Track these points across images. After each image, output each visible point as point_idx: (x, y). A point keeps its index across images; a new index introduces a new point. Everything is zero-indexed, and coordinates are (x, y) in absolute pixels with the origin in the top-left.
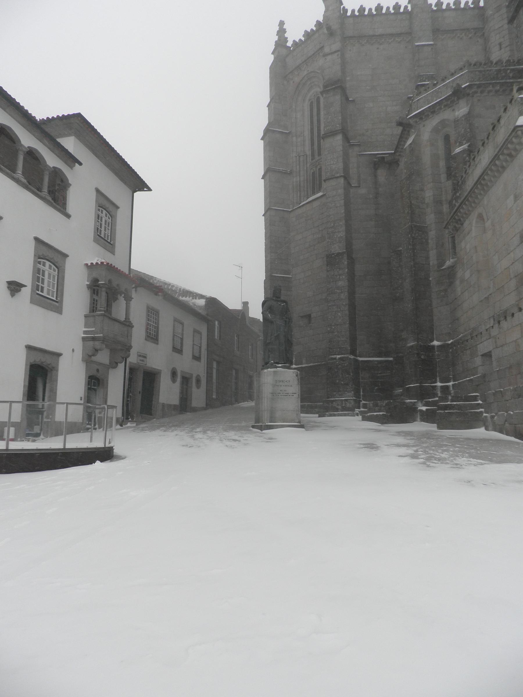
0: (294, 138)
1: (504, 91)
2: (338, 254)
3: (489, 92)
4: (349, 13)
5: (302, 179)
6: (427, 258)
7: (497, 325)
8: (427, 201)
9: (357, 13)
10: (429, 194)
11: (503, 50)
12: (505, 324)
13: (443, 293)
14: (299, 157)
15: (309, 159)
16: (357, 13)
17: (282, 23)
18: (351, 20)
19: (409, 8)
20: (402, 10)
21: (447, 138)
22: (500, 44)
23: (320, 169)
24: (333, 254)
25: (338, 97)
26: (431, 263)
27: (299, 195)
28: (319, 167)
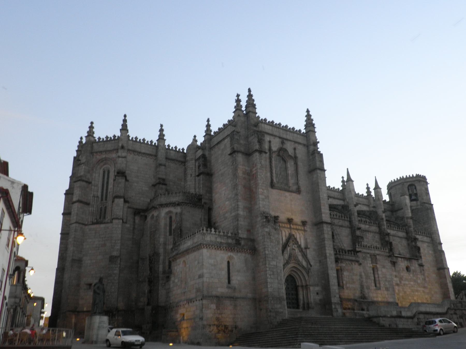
0: (93, 187)
1: (193, 207)
2: (116, 257)
3: (188, 206)
4: (130, 138)
5: (95, 209)
6: (159, 268)
7: (187, 304)
8: (160, 242)
9: (134, 139)
10: (162, 240)
11: (192, 178)
12: (190, 304)
13: (163, 284)
14: (95, 197)
15: (100, 199)
16: (134, 139)
17: (92, 123)
18: (131, 142)
19: (157, 144)
20: (153, 144)
21: (171, 218)
22: (191, 175)
23: (106, 207)
24: (113, 256)
25: (124, 180)
26: (160, 270)
27: (92, 217)
28: (105, 206)
